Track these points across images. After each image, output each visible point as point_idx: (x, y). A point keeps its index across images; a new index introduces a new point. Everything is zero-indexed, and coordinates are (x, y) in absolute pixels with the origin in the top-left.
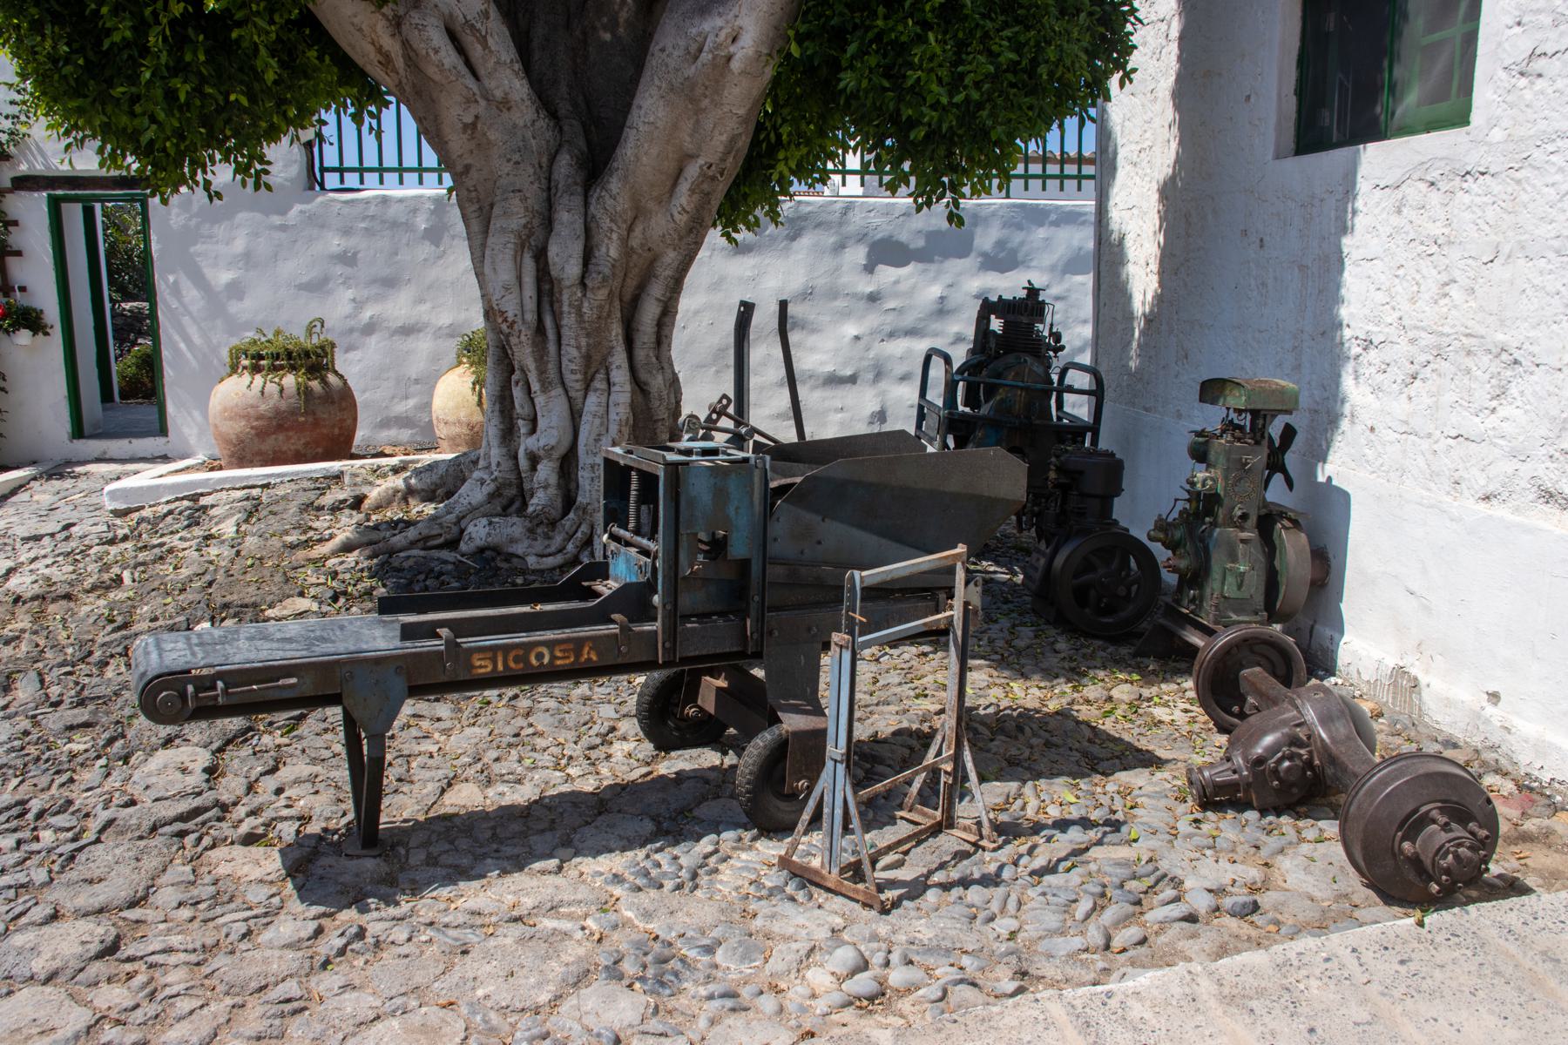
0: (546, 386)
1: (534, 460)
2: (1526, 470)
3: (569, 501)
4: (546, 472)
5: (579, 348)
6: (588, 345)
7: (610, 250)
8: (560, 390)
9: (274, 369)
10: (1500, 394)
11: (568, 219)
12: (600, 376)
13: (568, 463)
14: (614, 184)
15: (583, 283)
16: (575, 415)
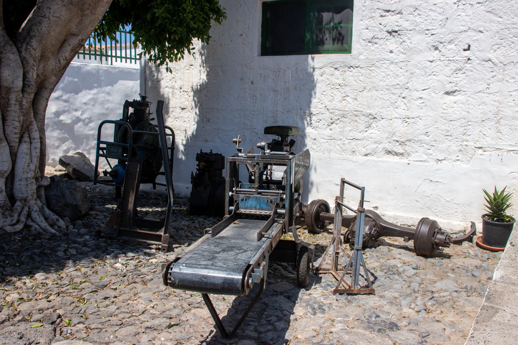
2: (381, 146)
5: (19, 122)
6: (23, 120)
7: (33, 75)
8: (6, 143)
10: (369, 126)
12: (26, 135)
14: (34, 43)
15: (23, 91)
16: (14, 156)
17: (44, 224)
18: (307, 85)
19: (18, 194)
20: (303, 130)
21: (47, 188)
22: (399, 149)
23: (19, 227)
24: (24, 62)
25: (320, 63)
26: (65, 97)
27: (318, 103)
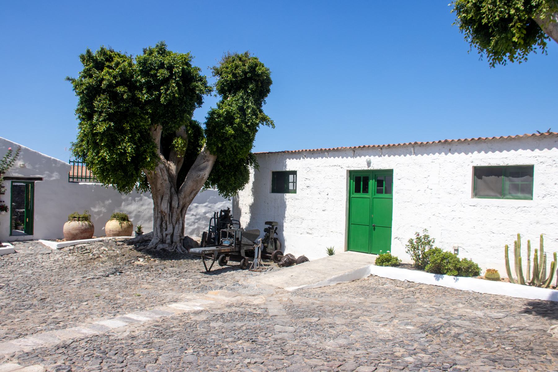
0: (170, 223)
1: (167, 235)
3: (172, 242)
4: (169, 237)
7: (181, 203)
9: (82, 220)
11: (175, 198)
13: (172, 235)
14: (182, 193)
16: (174, 228)
17: (180, 251)
18: (283, 206)
19: (174, 241)
20: (283, 223)
21: (184, 240)
22: (310, 232)
23: (173, 250)
24: (179, 199)
25: (287, 196)
26: (209, 205)
27: (287, 214)
